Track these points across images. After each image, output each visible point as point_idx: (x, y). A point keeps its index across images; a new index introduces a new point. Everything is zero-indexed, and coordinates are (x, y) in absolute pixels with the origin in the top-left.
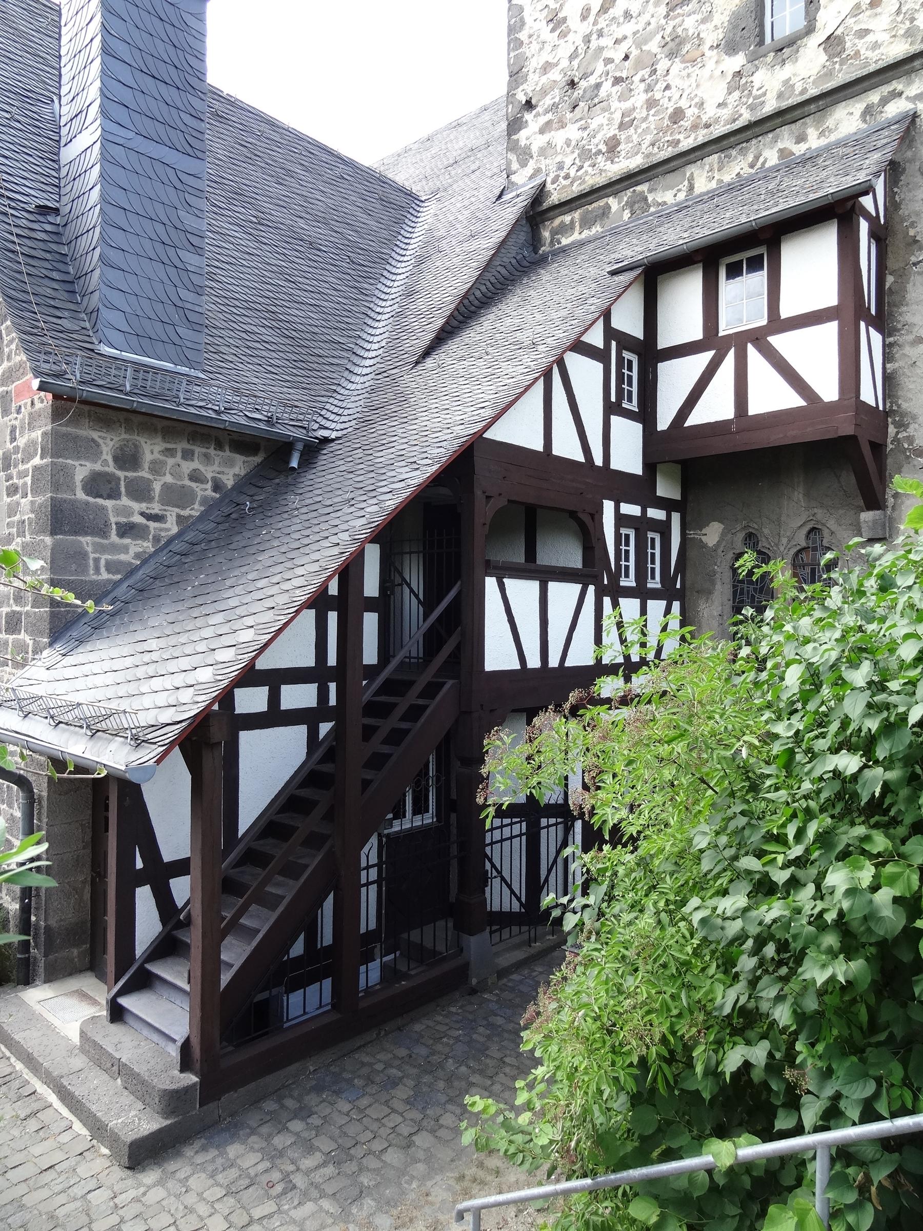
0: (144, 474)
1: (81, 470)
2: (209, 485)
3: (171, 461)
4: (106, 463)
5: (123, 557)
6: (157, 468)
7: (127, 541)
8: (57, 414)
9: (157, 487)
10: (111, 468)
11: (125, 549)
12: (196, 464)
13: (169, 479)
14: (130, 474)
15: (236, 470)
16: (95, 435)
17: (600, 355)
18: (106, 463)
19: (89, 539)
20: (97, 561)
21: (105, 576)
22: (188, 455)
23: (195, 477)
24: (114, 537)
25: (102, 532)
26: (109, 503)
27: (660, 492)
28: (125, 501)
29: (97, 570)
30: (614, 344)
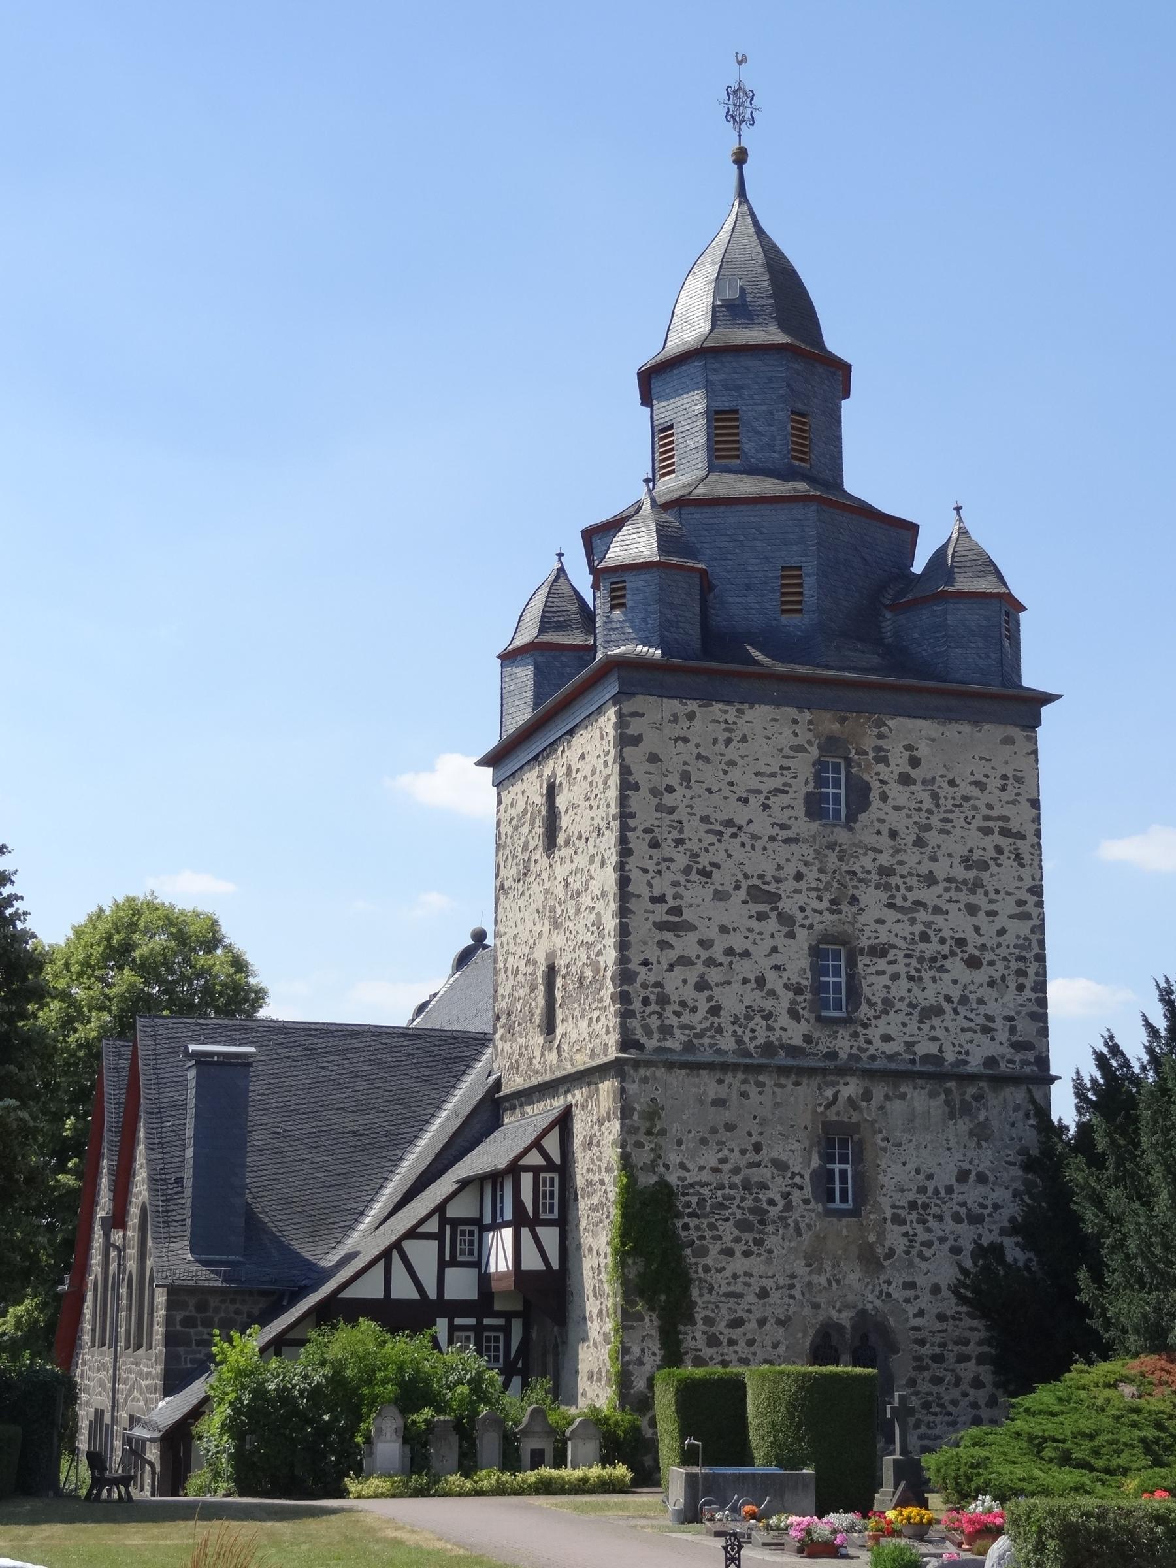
0: (210, 1314)
1: (179, 1316)
2: (245, 1316)
3: (223, 1306)
4: (191, 1311)
5: (198, 1356)
6: (217, 1310)
7: (200, 1348)
8: (168, 1294)
9: (216, 1320)
10: (194, 1313)
11: (200, 1352)
12: (238, 1306)
13: (223, 1315)
14: (203, 1315)
15: (261, 1306)
16: (186, 1298)
17: (439, 1237)
18: (191, 1311)
19: (181, 1348)
20: (185, 1358)
21: (189, 1366)
22: (233, 1301)
23: (237, 1312)
24: (194, 1347)
25: (188, 1344)
26: (192, 1330)
27: (496, 1308)
28: (200, 1328)
29: (186, 1362)
30: (448, 1227)
